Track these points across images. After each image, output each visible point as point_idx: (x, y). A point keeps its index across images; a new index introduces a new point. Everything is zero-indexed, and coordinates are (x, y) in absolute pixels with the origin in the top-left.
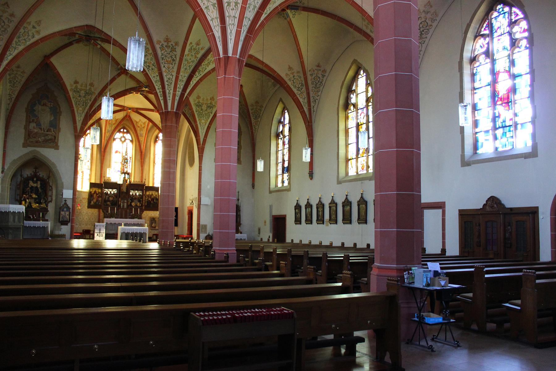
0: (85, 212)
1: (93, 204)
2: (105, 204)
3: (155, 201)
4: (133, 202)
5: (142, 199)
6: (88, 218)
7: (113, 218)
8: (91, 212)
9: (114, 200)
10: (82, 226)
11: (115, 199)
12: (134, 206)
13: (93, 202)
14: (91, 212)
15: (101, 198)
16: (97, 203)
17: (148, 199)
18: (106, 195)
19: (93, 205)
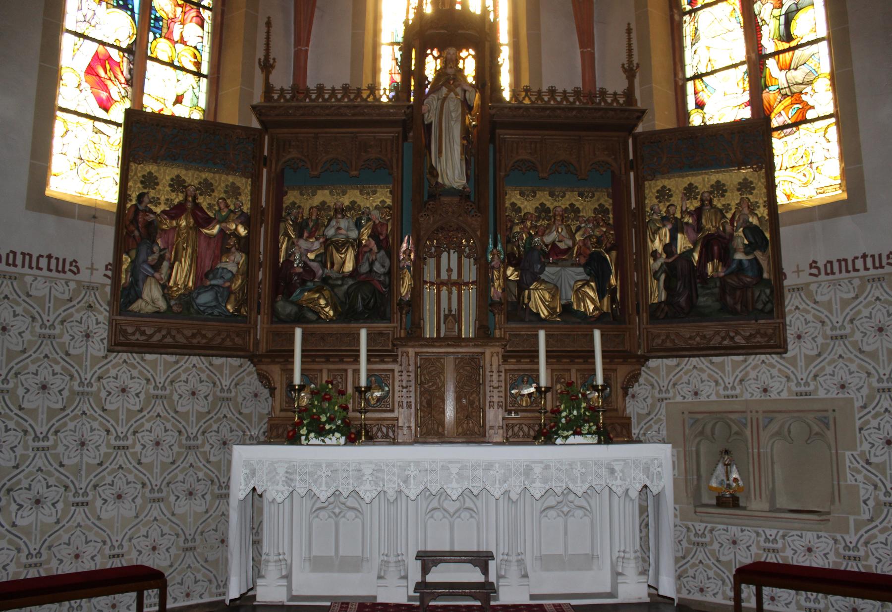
0: (135, 386)
1: (162, 305)
2: (285, 308)
3: (739, 256)
4: (536, 278)
5: (614, 253)
6: (170, 438)
7: (321, 432)
8: (203, 389)
9: (365, 268)
10: (109, 512)
11: (371, 264)
12: (544, 313)
13: (164, 287)
14: (203, 389)
15: (241, 258)
16: (205, 298)
17: (669, 248)
18: (300, 236)
19: (157, 313)
